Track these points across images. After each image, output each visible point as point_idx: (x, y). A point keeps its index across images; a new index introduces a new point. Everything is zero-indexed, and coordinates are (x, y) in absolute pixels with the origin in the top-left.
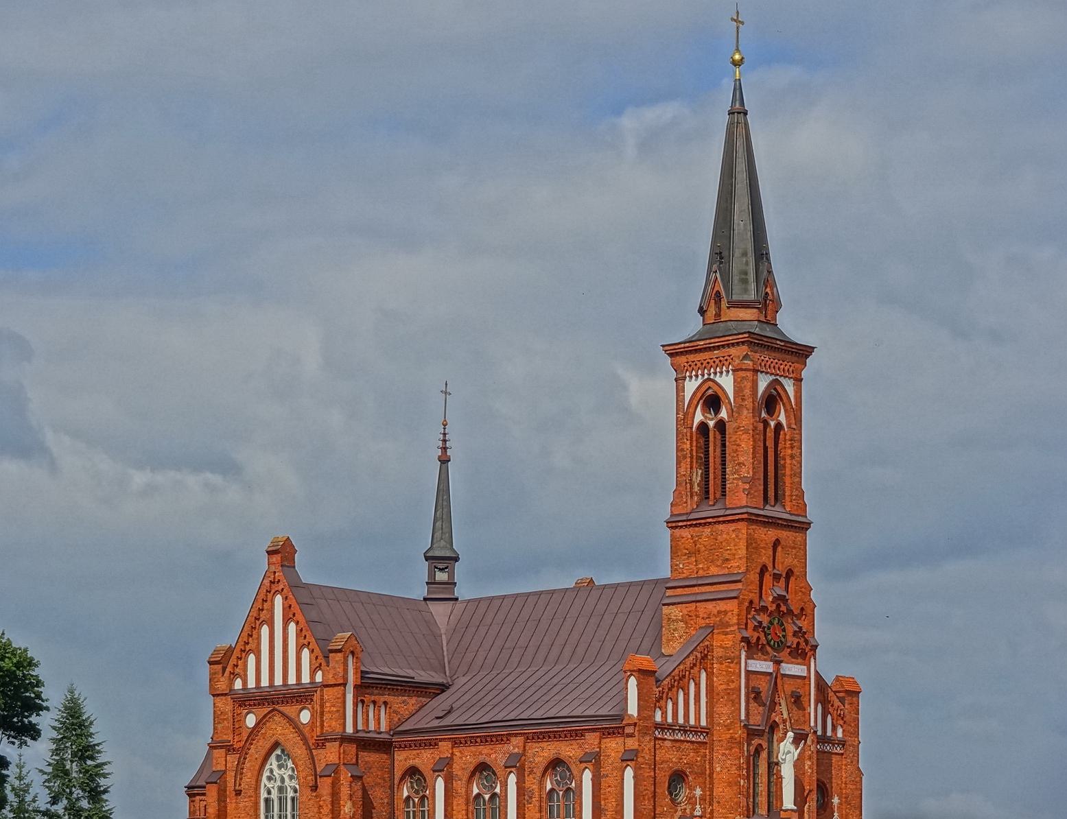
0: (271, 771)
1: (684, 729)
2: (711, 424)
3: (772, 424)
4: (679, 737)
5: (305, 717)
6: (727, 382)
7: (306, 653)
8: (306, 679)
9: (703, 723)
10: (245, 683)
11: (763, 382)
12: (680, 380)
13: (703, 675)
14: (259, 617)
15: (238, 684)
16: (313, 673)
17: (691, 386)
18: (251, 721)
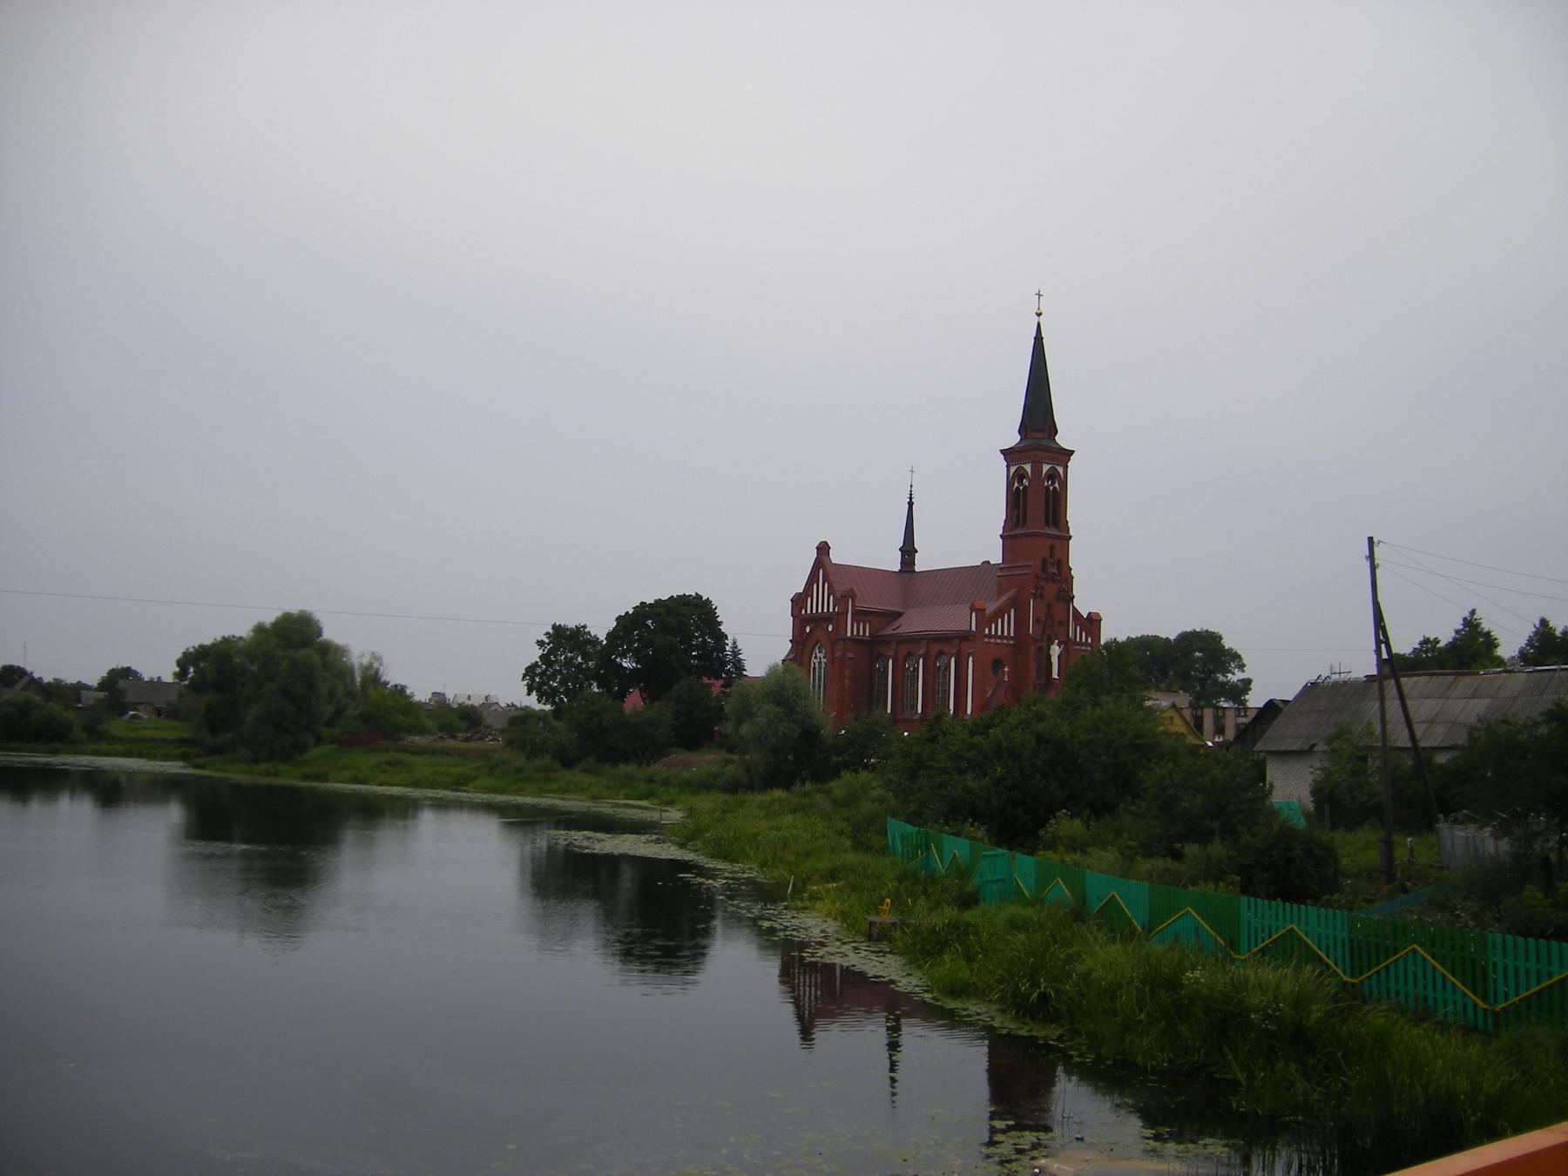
1: (1002, 637)
2: (1021, 488)
3: (1051, 488)
5: (830, 628)
6: (1028, 468)
7: (831, 597)
8: (831, 610)
9: (1012, 635)
10: (806, 611)
11: (1046, 468)
13: (1013, 610)
14: (813, 578)
15: (803, 612)
16: (834, 609)
17: (1013, 469)
18: (808, 630)
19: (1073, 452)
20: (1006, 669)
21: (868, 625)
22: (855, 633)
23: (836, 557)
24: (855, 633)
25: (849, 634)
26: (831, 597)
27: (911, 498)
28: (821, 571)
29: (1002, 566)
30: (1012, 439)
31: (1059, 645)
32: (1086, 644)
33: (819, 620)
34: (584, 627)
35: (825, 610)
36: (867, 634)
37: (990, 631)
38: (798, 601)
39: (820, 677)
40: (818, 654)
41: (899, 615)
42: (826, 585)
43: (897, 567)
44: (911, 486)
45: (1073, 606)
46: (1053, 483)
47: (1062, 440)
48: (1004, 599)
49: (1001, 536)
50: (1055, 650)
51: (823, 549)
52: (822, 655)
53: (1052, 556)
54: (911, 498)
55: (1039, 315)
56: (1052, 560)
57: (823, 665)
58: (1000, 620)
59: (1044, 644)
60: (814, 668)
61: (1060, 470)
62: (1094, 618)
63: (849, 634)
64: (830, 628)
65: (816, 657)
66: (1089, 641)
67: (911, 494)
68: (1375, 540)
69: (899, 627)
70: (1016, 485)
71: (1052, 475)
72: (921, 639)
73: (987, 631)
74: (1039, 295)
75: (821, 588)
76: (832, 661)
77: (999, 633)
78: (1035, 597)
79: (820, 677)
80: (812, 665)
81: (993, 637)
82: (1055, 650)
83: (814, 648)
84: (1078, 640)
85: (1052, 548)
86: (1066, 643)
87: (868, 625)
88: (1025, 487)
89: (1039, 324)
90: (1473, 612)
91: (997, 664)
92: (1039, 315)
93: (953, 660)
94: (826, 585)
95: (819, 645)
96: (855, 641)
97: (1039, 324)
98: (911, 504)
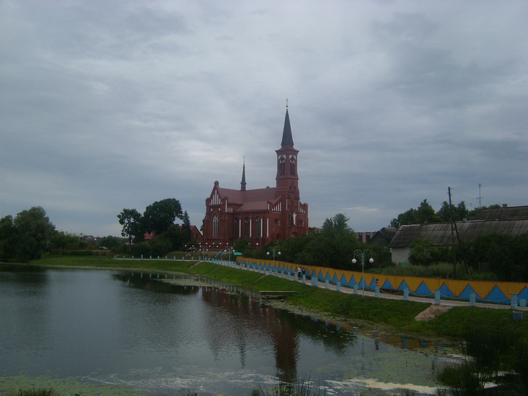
1: (277, 212)
2: (282, 163)
4: (276, 213)
5: (220, 209)
6: (285, 156)
7: (220, 199)
8: (220, 203)
9: (281, 211)
10: (211, 204)
11: (290, 156)
12: (278, 156)
13: (281, 203)
14: (213, 193)
15: (210, 204)
16: (221, 203)
17: (280, 157)
18: (212, 210)
19: (299, 151)
20: (279, 222)
21: (232, 208)
22: (228, 211)
23: (221, 186)
24: (228, 211)
25: (226, 211)
26: (220, 199)
27: (244, 166)
28: (216, 191)
29: (276, 188)
30: (279, 147)
31: (296, 214)
32: (304, 214)
33: (215, 207)
34: (135, 210)
35: (218, 204)
36: (232, 211)
37: (274, 210)
38: (208, 201)
39: (216, 225)
40: (215, 218)
41: (242, 205)
42: (218, 195)
43: (240, 189)
44: (244, 162)
45: (300, 202)
46: (292, 161)
47: (295, 147)
48: (277, 200)
49: (276, 179)
50: (295, 216)
51: (217, 183)
52: (217, 218)
53: (292, 185)
54: (244, 166)
55: (287, 107)
56: (293, 186)
57: (217, 222)
58: (277, 206)
59: (291, 214)
60: (214, 223)
61: (295, 157)
62: (306, 205)
63: (226, 211)
64: (220, 209)
65: (215, 219)
66: (304, 212)
67: (244, 165)
68: (450, 188)
69: (242, 209)
70: (281, 162)
71: (293, 159)
72: (251, 213)
74: (287, 100)
75: (216, 197)
76: (220, 220)
77: (277, 210)
78: (288, 198)
79: (216, 225)
80: (214, 222)
81: (276, 211)
82: (295, 216)
83: (214, 216)
84: (301, 212)
85: (293, 182)
86: (298, 213)
87: (232, 208)
88: (284, 163)
89: (287, 110)
90: (425, 201)
91: (276, 220)
92: (287, 107)
93: (262, 219)
94: (218, 195)
95: (216, 215)
96: (228, 213)
97: (287, 110)
98: (244, 168)
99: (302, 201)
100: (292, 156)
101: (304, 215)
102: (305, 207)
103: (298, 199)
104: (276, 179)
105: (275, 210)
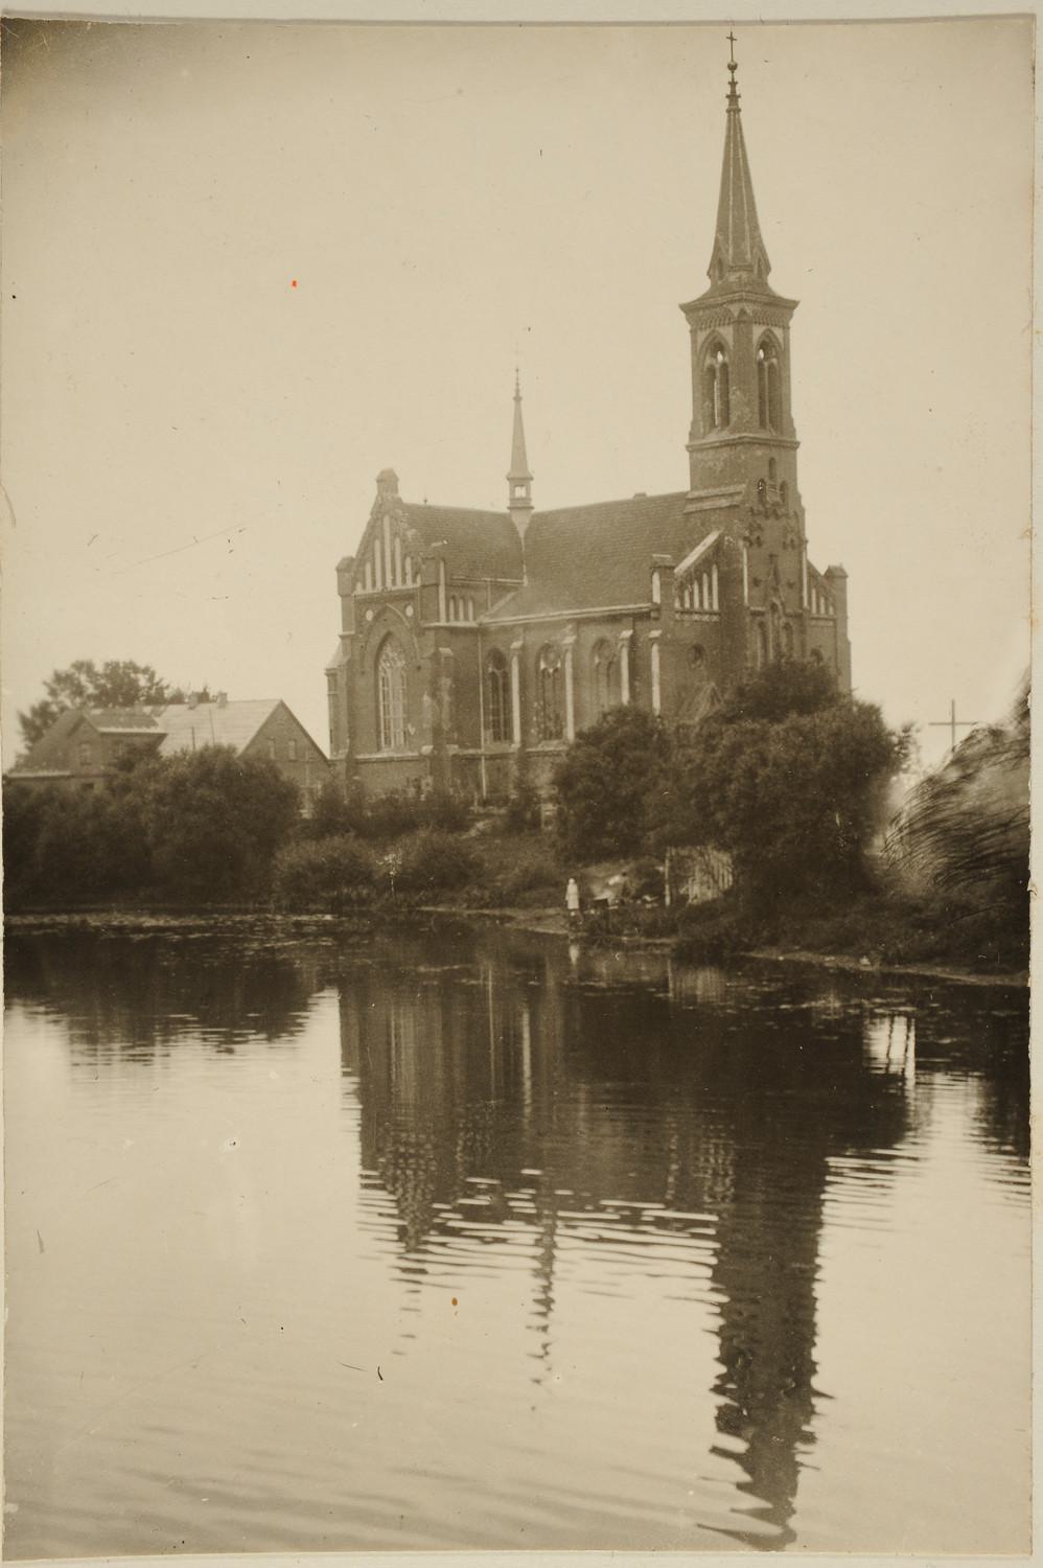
0: (387, 656)
6: (727, 333)
9: (716, 607)
11: (758, 332)
12: (693, 332)
17: (702, 336)
18: (369, 615)
26: (408, 561)
27: (518, 391)
30: (699, 285)
38: (350, 571)
49: (687, 447)
51: (387, 481)
61: (778, 332)
73: (677, 605)
81: (690, 612)
84: (814, 610)
85: (772, 462)
87: (470, 605)
98: (518, 399)
99: (819, 556)
100: (764, 328)
101: (831, 623)
102: (832, 582)
103: (798, 544)
104: (687, 447)
105: (687, 605)
